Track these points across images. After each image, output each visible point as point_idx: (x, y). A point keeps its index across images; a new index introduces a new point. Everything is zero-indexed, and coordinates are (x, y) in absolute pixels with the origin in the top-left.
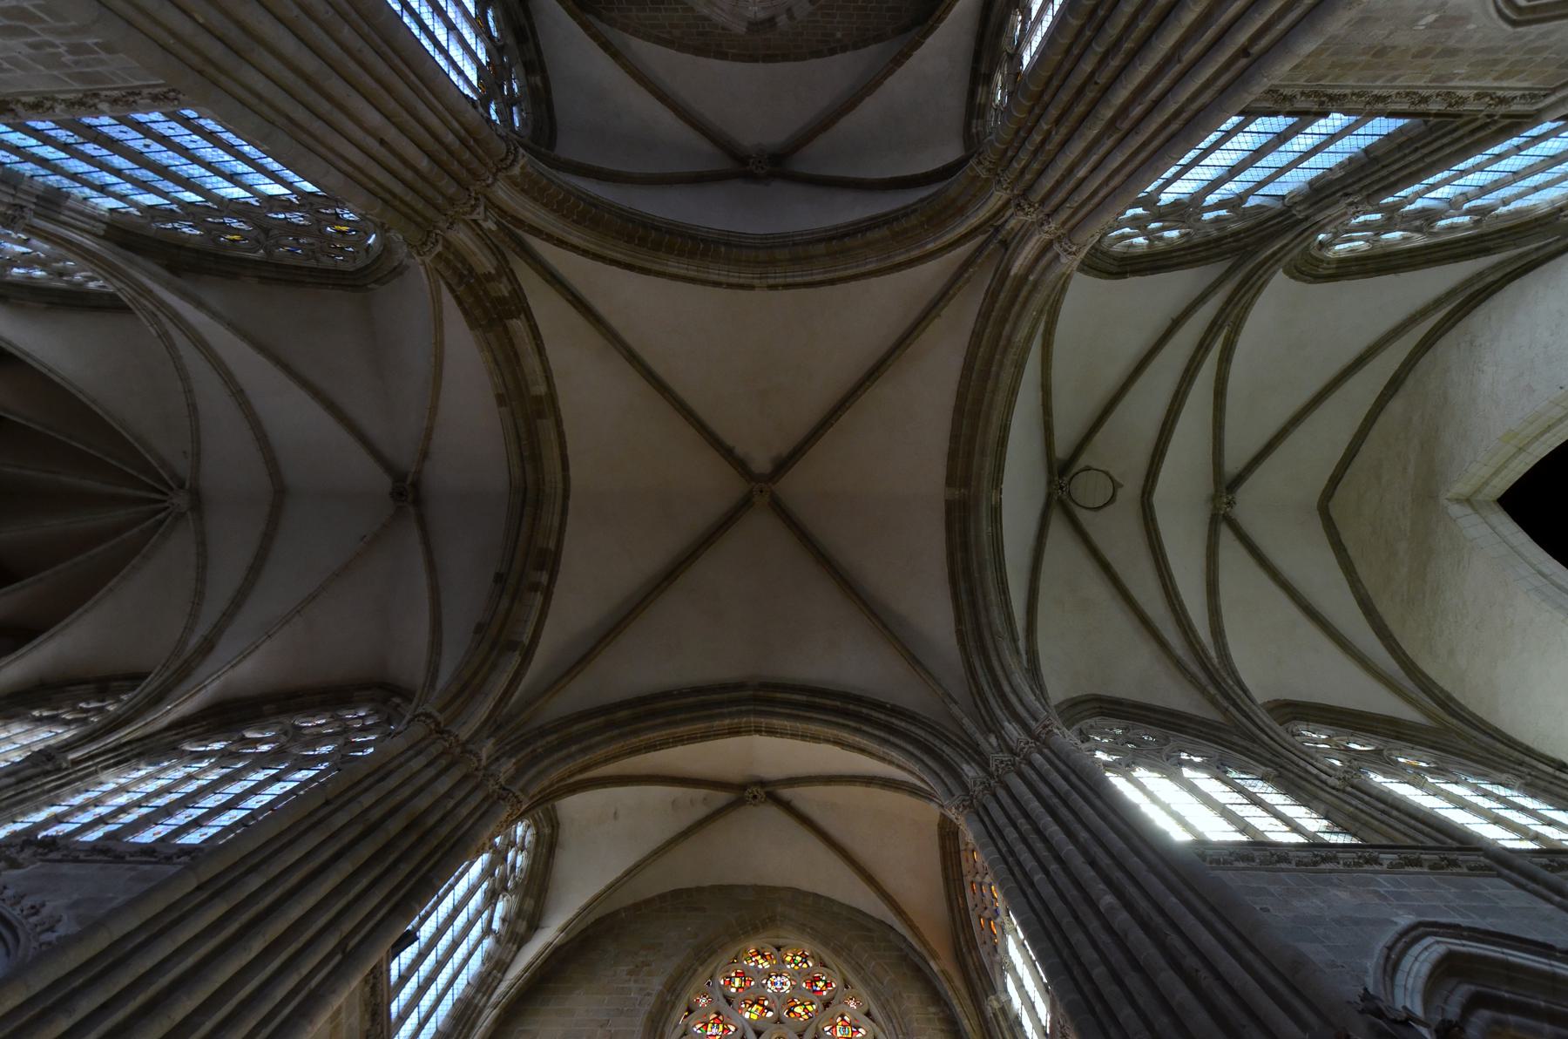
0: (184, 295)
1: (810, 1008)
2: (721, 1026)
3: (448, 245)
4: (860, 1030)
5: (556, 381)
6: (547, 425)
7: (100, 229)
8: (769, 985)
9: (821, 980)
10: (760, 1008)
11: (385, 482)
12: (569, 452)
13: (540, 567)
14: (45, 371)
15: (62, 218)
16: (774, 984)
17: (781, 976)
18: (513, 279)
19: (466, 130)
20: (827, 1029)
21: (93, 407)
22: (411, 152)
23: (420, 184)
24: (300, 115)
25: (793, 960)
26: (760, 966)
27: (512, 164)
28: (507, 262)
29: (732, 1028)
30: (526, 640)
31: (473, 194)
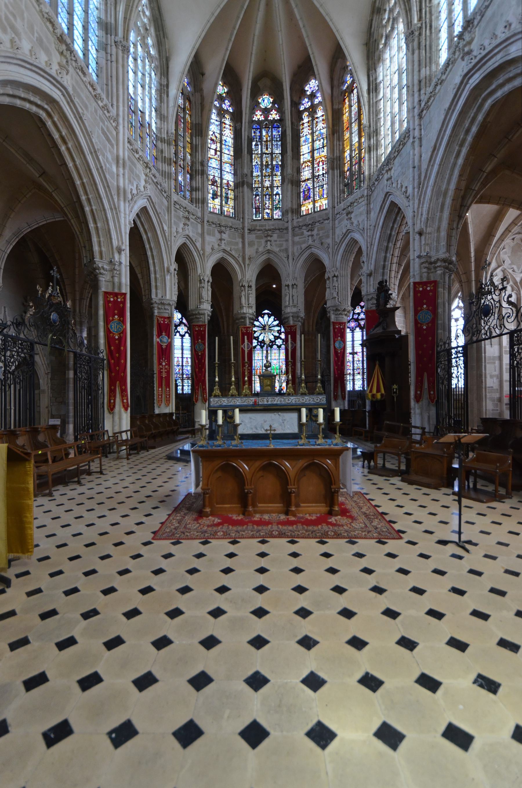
15: (113, 22)
21: (216, 14)
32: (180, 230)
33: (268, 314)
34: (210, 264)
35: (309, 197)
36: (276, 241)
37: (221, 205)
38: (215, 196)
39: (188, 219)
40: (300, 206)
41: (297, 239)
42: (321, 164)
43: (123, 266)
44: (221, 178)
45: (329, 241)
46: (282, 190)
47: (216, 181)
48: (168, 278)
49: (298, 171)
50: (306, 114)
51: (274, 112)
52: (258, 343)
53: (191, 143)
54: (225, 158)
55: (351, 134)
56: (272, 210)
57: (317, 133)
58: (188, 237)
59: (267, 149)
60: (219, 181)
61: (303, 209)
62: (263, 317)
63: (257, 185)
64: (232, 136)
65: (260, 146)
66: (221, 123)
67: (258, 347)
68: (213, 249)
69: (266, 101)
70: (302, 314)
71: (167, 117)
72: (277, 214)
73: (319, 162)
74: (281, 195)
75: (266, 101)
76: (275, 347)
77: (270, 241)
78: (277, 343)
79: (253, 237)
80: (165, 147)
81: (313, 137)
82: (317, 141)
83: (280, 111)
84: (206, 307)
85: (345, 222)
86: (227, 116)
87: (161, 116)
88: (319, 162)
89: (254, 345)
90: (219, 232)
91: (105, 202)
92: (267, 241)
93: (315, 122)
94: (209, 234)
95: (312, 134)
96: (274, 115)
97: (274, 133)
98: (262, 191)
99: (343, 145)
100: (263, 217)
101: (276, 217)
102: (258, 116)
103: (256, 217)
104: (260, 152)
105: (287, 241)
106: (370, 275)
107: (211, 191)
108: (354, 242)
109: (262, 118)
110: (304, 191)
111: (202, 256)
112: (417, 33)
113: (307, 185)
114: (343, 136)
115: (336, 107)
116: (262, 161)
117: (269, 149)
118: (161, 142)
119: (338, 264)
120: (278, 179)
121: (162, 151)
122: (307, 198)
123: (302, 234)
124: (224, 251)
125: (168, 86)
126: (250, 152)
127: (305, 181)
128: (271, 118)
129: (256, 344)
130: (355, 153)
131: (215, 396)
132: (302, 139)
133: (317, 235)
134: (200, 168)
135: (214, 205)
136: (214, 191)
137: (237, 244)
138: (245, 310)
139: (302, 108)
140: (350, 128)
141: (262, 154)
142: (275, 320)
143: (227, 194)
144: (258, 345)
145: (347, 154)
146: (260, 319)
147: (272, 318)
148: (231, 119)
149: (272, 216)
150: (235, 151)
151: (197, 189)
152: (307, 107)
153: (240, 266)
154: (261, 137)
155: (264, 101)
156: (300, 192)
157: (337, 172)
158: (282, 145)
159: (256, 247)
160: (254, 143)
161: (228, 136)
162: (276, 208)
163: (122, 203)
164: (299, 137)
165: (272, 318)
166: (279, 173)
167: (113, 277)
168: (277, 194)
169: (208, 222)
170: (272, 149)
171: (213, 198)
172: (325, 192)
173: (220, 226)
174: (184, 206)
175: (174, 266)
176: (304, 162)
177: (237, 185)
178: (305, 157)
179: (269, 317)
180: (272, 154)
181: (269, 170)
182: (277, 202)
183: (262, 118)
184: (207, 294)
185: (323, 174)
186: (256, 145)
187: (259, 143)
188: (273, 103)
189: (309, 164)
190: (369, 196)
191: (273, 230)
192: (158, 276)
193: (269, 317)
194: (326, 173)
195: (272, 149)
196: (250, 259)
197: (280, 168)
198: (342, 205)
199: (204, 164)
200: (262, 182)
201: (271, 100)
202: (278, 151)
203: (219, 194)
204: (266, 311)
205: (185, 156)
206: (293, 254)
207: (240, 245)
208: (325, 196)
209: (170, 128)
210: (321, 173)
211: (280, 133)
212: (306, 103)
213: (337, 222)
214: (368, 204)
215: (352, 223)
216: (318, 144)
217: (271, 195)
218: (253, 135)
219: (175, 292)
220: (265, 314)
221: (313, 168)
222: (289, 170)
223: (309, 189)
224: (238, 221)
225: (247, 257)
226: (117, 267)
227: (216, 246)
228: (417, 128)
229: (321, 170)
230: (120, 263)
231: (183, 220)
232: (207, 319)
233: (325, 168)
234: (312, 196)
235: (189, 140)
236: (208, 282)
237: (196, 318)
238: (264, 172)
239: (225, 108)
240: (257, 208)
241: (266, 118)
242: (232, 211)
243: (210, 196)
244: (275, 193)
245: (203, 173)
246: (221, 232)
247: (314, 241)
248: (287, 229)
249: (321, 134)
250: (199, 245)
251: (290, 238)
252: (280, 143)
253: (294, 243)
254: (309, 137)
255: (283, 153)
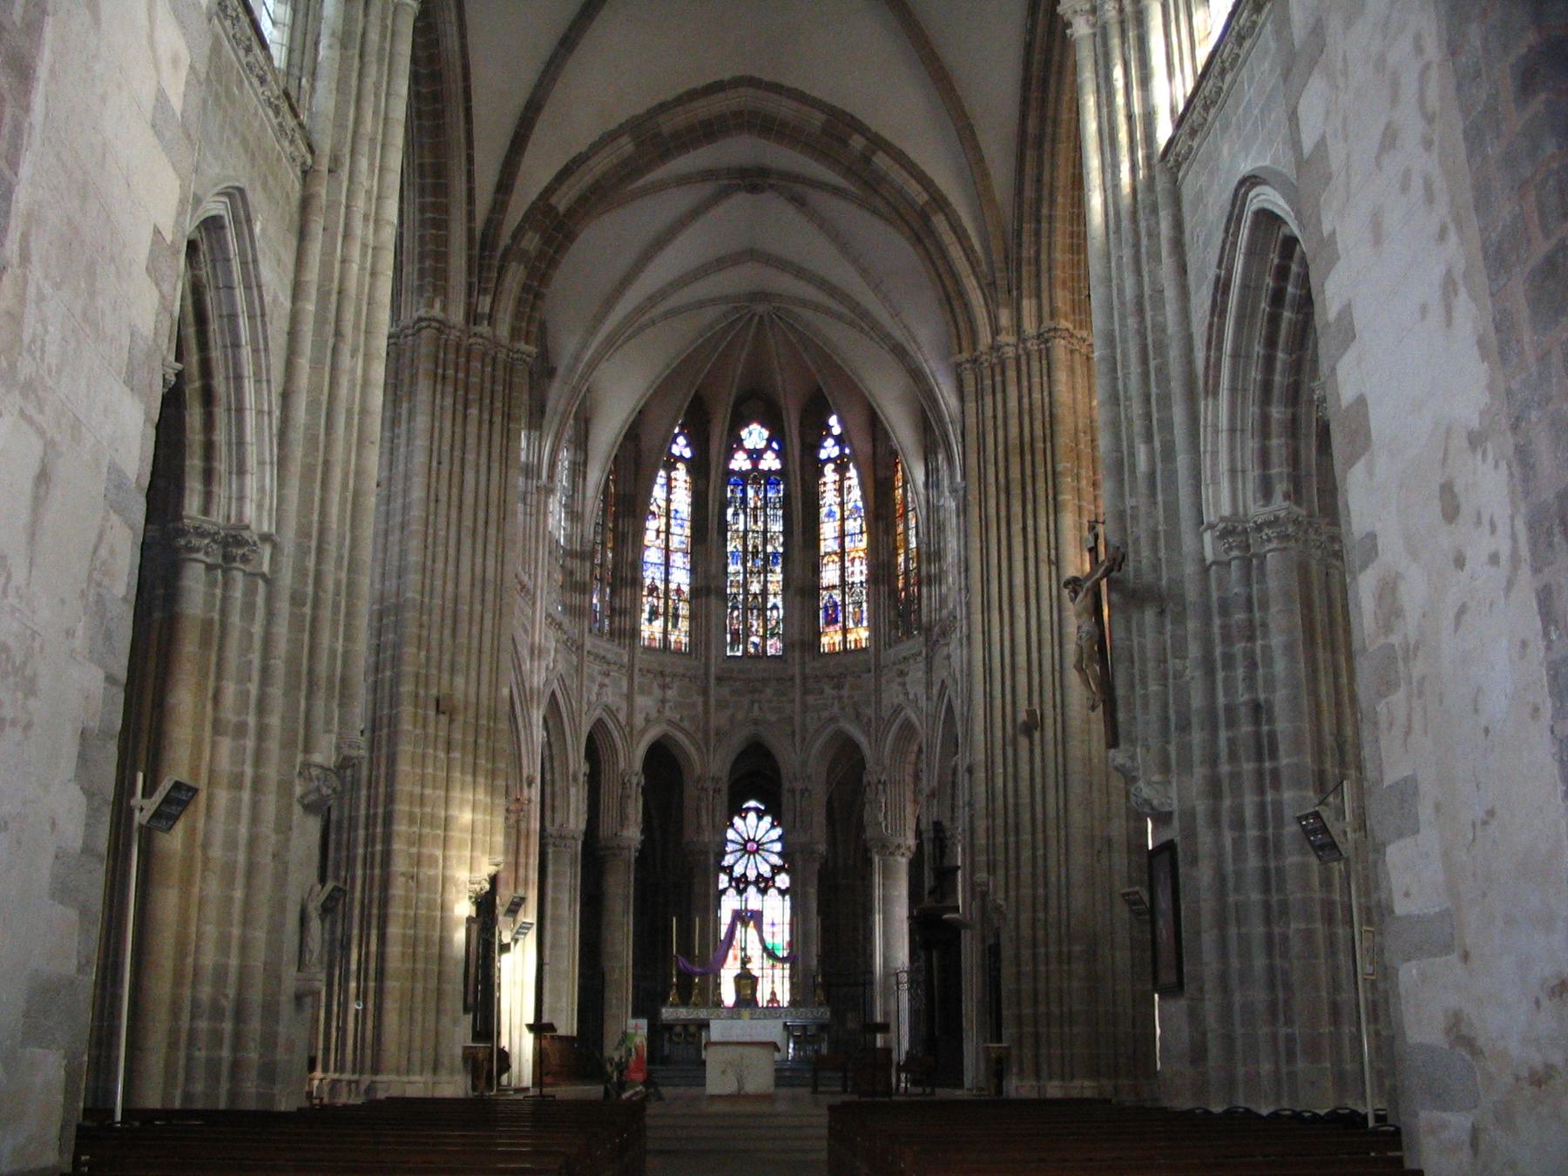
0: (571, 369)
3: (515, 333)
5: (612, 126)
6: (667, 124)
7: (536, 434)
11: (741, 199)
12: (699, 82)
13: (844, 142)
14: (643, 402)
18: (518, 234)
19: (435, 382)
22: (472, 429)
23: (487, 401)
24: (492, 531)
27: (438, 321)
28: (507, 250)
30: (923, 198)
31: (472, 341)
32: (593, 698)
33: (757, 810)
34: (640, 752)
35: (836, 621)
36: (771, 701)
37: (665, 632)
38: (654, 614)
39: (608, 675)
40: (818, 635)
41: (810, 699)
42: (857, 562)
43: (532, 805)
44: (667, 581)
45: (870, 712)
46: (784, 600)
47: (657, 588)
48: (573, 790)
49: (816, 570)
50: (829, 468)
51: (769, 455)
52: (730, 882)
53: (615, 530)
54: (675, 542)
55: (907, 529)
56: (764, 638)
57: (851, 505)
58: (607, 708)
59: (756, 522)
60: (661, 587)
61: (825, 640)
62: (744, 818)
63: (734, 590)
64: (689, 500)
65: (742, 517)
66: (669, 479)
67: (732, 892)
68: (647, 720)
69: (755, 434)
70: (822, 848)
71: (583, 513)
72: (774, 647)
73: (854, 559)
74: (781, 611)
75: (755, 435)
76: (772, 892)
77: (760, 702)
78: (777, 885)
79: (725, 691)
80: (577, 564)
81: (842, 511)
82: (851, 520)
83: (780, 454)
84: (633, 834)
85: (895, 687)
86: (680, 466)
87: (574, 515)
88: (854, 559)
89: (721, 886)
90: (659, 686)
91: (520, 720)
92: (752, 702)
93: (847, 483)
94: (642, 692)
95: (842, 504)
96: (770, 462)
97: (769, 495)
98: (745, 599)
99: (895, 541)
100: (745, 650)
101: (771, 651)
102: (740, 462)
103: (732, 649)
104: (741, 528)
105: (793, 701)
106: (932, 795)
107: (647, 608)
108: (908, 729)
109: (747, 465)
110: (826, 608)
111: (630, 734)
112: (961, 493)
113: (831, 597)
114: (895, 526)
115: (881, 473)
116: (745, 545)
117: (760, 524)
118: (572, 557)
119: (887, 761)
120: (776, 577)
121: (571, 573)
122: (832, 621)
123: (822, 692)
124: (670, 722)
125: (585, 464)
126: (723, 526)
127: (827, 588)
128: (763, 465)
129: (726, 885)
130: (913, 565)
131: (672, 1005)
132: (824, 511)
133: (850, 697)
134: (629, 575)
135: (651, 630)
136: (652, 607)
137: (694, 705)
138: (707, 837)
139: (823, 455)
140: (905, 515)
141: (746, 532)
142: (773, 826)
143: (676, 609)
144: (730, 885)
145: (901, 559)
146: (737, 821)
147: (768, 820)
148: (689, 472)
149: (765, 651)
150: (692, 528)
151: (622, 612)
152: (833, 456)
153: (698, 749)
154: (744, 501)
155: (750, 433)
156: (818, 608)
157: (884, 589)
158: (784, 517)
159: (729, 712)
160: (730, 511)
161: (682, 501)
162: (773, 635)
163: (535, 711)
164: (818, 507)
165: (768, 820)
166: (778, 569)
167: (518, 821)
168: (775, 607)
169: (640, 670)
170: (765, 523)
171: (650, 621)
172: (865, 615)
173: (662, 674)
174: (602, 653)
175: (584, 768)
176: (827, 554)
177: (695, 591)
178: (828, 543)
179: (760, 818)
180: (765, 531)
181: (760, 563)
182: (774, 623)
183: (747, 465)
184: (635, 810)
185: (861, 582)
186: (736, 514)
187: (740, 511)
188: (769, 441)
189: (836, 559)
190: (929, 661)
191: (765, 682)
192: (557, 789)
193: (760, 818)
194: (867, 581)
195: (765, 523)
196: (717, 734)
197: (780, 560)
198: (891, 654)
199: (637, 565)
200: (745, 584)
201: (766, 434)
202: (777, 527)
203: (661, 610)
204: (752, 804)
205: (604, 555)
206: (804, 725)
207: (700, 709)
208: (865, 623)
209: (586, 534)
210: (858, 578)
211: (781, 494)
212: (829, 450)
213: (883, 680)
214: (929, 670)
215: (907, 694)
216: (853, 525)
217: (763, 610)
218: (729, 495)
219: (583, 818)
220: (748, 810)
221: (843, 569)
222: (797, 571)
223: (835, 604)
224: (695, 663)
225: (712, 733)
226: (525, 807)
227: (654, 714)
228: (964, 622)
229: (858, 572)
230: (530, 801)
231: (599, 679)
232: (633, 855)
233: (865, 572)
234: (840, 619)
235: (611, 525)
236: (638, 784)
237: (615, 855)
238: (749, 564)
239: (678, 454)
240: (735, 633)
241: (755, 463)
242: (685, 640)
243: (645, 615)
244: (769, 605)
245: (636, 582)
246: (664, 687)
247: (843, 708)
248: (792, 679)
249: (856, 508)
250: (622, 717)
251: (797, 699)
252: (780, 513)
253: (805, 708)
254: (836, 509)
255: (787, 532)
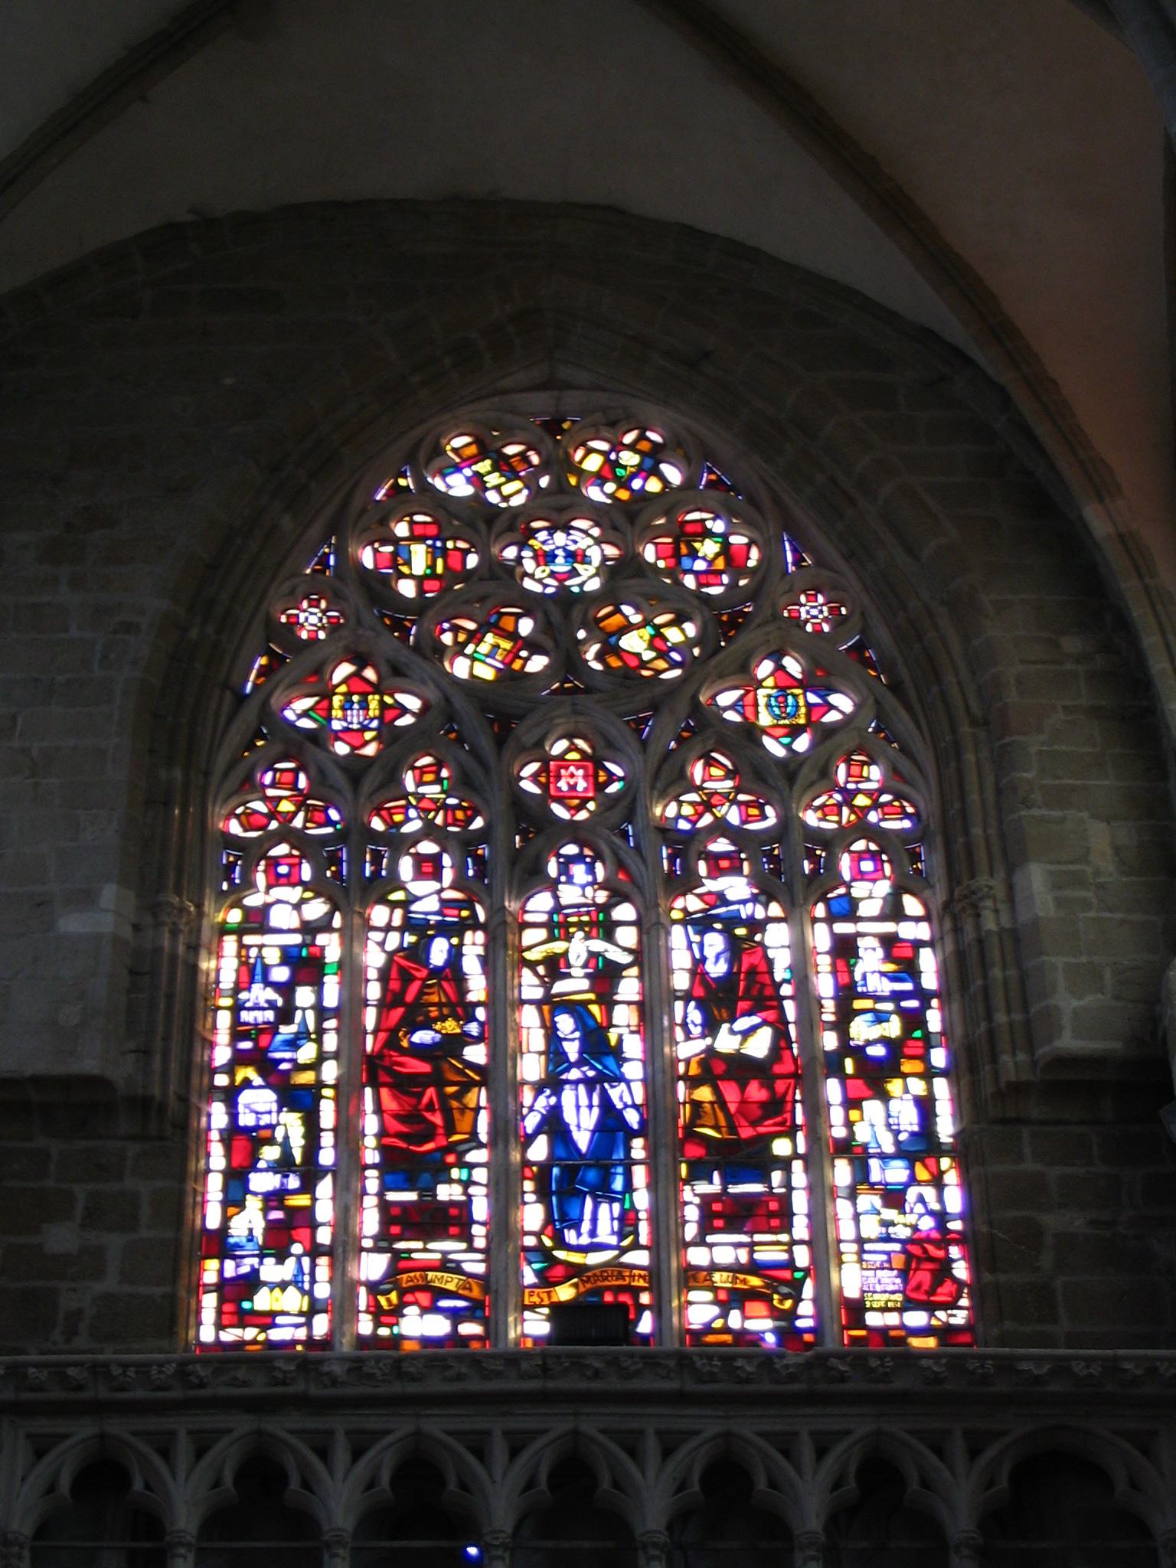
1: (673, 635)
2: (374, 701)
4: (835, 699)
8: (529, 565)
9: (708, 534)
10: (506, 645)
16: (549, 558)
17: (567, 529)
20: (726, 699)
25: (612, 465)
26: (492, 497)
29: (413, 703)
